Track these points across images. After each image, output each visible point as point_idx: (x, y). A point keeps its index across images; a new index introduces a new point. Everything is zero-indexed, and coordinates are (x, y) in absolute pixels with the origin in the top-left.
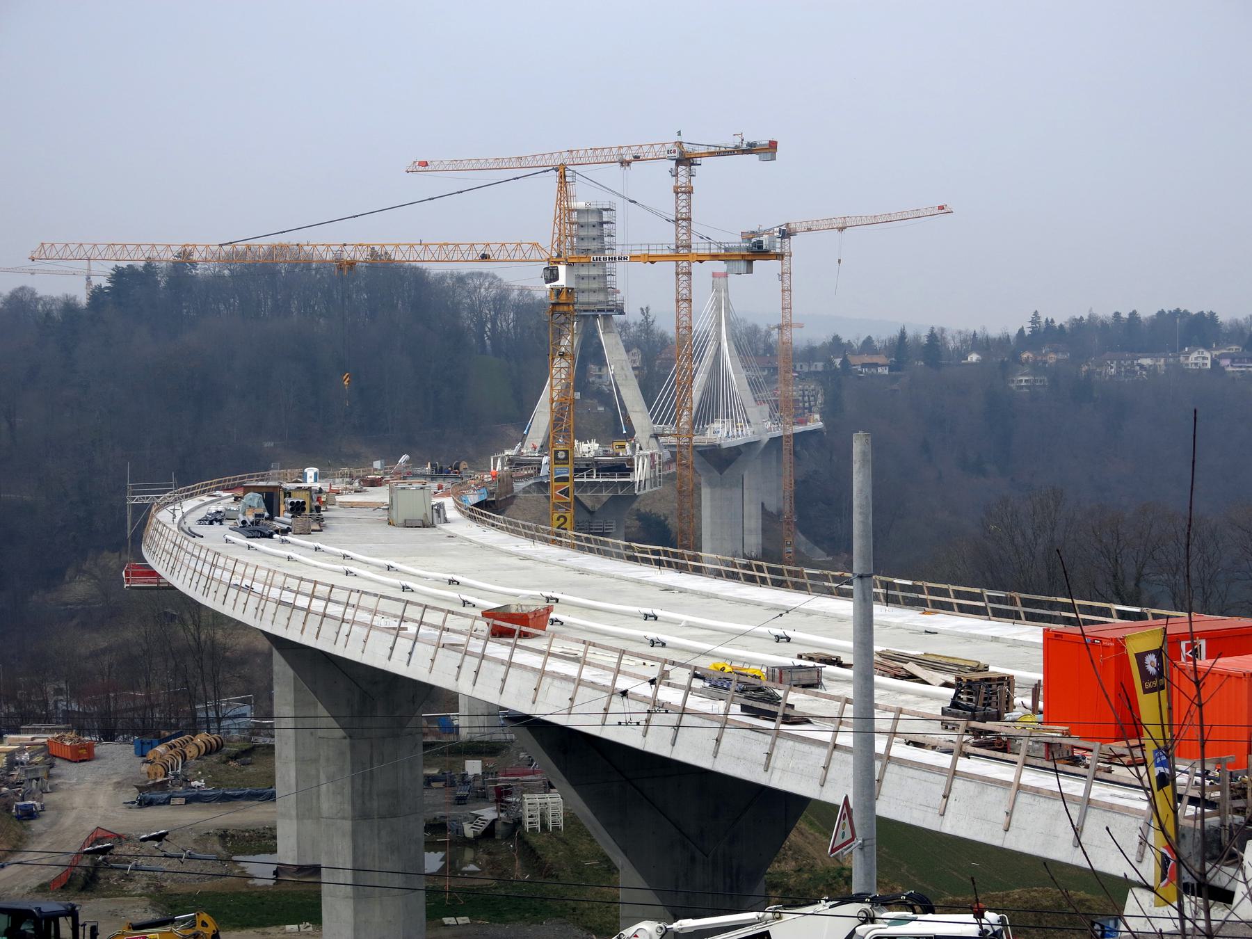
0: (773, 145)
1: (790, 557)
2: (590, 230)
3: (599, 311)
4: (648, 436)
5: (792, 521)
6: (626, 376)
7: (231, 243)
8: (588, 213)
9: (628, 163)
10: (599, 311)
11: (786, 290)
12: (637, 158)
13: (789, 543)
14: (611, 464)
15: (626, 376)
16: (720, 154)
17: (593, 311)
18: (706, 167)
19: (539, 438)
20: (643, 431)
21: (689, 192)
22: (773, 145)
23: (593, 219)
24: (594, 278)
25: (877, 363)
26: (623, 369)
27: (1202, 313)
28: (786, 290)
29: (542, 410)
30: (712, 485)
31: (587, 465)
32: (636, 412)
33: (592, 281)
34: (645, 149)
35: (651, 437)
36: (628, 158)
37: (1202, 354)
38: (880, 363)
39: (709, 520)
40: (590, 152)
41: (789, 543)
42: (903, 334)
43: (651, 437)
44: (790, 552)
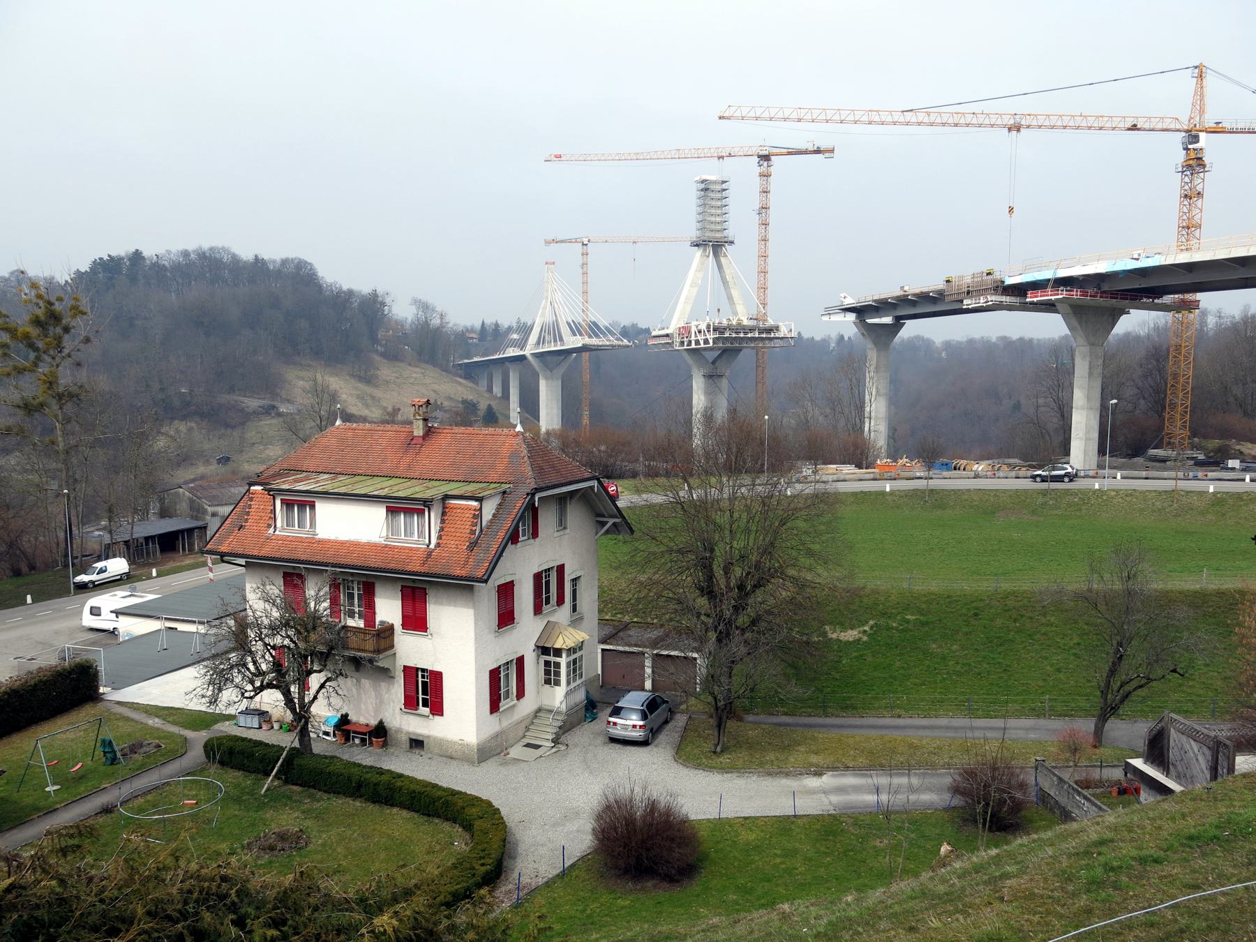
0: (832, 151)
9: (722, 157)
10: (725, 242)
11: (585, 273)
12: (730, 155)
16: (790, 154)
21: (768, 175)
22: (832, 151)
23: (718, 187)
28: (585, 273)
30: (546, 378)
34: (737, 150)
36: (724, 155)
39: (545, 398)
40: (693, 151)
42: (483, 322)
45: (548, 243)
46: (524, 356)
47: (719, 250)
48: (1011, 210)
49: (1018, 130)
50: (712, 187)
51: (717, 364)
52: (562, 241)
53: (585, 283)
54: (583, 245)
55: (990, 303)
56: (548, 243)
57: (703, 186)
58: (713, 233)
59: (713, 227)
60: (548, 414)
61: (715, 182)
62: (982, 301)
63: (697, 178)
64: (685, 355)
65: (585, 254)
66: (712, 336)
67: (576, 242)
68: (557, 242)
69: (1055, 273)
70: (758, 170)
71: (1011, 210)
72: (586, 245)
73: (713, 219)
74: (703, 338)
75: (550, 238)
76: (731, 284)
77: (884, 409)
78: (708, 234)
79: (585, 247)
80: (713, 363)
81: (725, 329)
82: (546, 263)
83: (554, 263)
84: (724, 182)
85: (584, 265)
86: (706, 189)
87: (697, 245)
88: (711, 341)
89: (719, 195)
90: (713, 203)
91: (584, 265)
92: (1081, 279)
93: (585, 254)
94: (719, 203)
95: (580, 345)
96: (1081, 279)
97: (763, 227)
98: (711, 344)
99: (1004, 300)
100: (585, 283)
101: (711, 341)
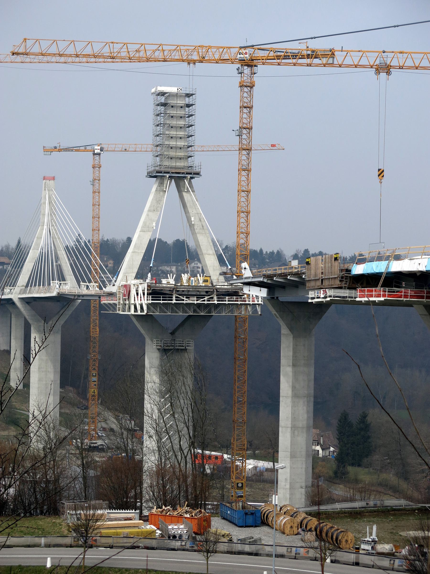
1: (95, 385)
2: (178, 110)
3: (187, 173)
4: (218, 274)
5: (97, 359)
6: (203, 226)
7: (253, 46)
8: (177, 99)
10: (187, 173)
13: (94, 374)
14: (226, 292)
15: (203, 226)
17: (183, 173)
18: (260, 69)
19: (133, 273)
20: (214, 270)
23: (181, 102)
24: (180, 148)
25: (4, 262)
26: (200, 220)
27: (166, 243)
29: (137, 251)
31: (207, 292)
32: (209, 254)
33: (178, 150)
35: (220, 274)
37: (197, 265)
38: (6, 262)
41: (94, 374)
43: (220, 274)
44: (95, 381)
45: (48, 151)
46: (10, 300)
47: (181, 183)
48: (381, 173)
49: (388, 73)
50: (172, 102)
51: (177, 334)
52: (67, 150)
53: (96, 205)
54: (94, 154)
55: (328, 299)
56: (48, 151)
57: (162, 99)
58: (174, 160)
59: (172, 153)
60: (40, 380)
61: (176, 95)
62: (322, 296)
63: (153, 90)
64: (134, 320)
65: (96, 167)
66: (146, 302)
67: (85, 150)
68: (60, 150)
69: (388, 267)
70: (237, 79)
71: (381, 173)
72: (99, 154)
73: (173, 143)
74: (139, 302)
75: (50, 145)
76: (197, 229)
77: (305, 416)
78: (167, 163)
79: (97, 157)
80: (173, 333)
81: (172, 291)
82: (44, 178)
83: (54, 178)
84: (188, 95)
85: (95, 180)
86: (164, 105)
87: (151, 177)
88: (145, 307)
89: (181, 112)
90: (174, 122)
91: (95, 180)
92: (418, 274)
93: (96, 167)
94: (181, 123)
95: (54, 294)
96: (418, 274)
97: (244, 152)
98: (146, 312)
99: (347, 295)
100: (96, 205)
101: (145, 307)
